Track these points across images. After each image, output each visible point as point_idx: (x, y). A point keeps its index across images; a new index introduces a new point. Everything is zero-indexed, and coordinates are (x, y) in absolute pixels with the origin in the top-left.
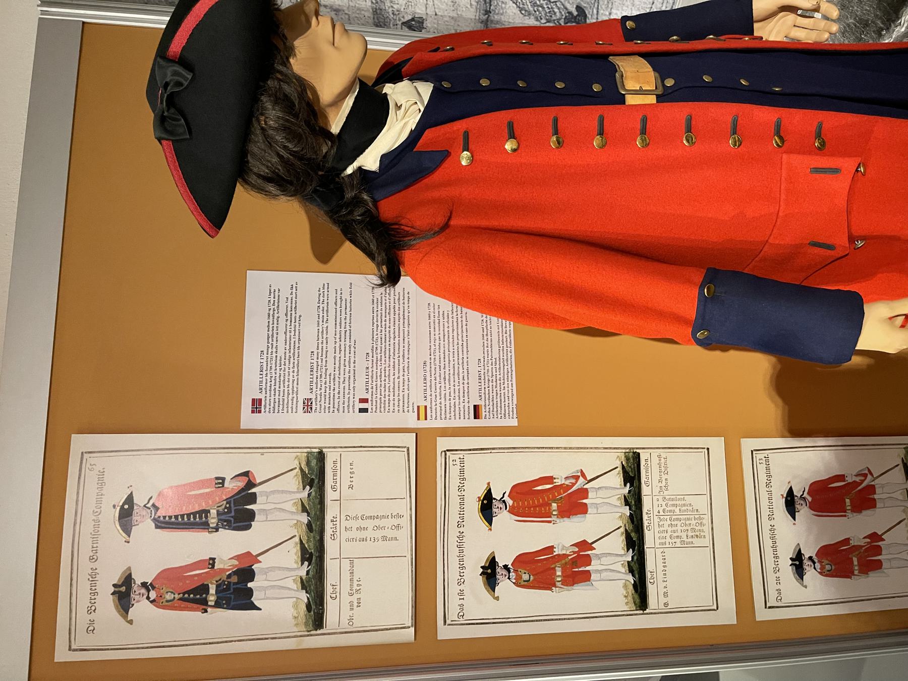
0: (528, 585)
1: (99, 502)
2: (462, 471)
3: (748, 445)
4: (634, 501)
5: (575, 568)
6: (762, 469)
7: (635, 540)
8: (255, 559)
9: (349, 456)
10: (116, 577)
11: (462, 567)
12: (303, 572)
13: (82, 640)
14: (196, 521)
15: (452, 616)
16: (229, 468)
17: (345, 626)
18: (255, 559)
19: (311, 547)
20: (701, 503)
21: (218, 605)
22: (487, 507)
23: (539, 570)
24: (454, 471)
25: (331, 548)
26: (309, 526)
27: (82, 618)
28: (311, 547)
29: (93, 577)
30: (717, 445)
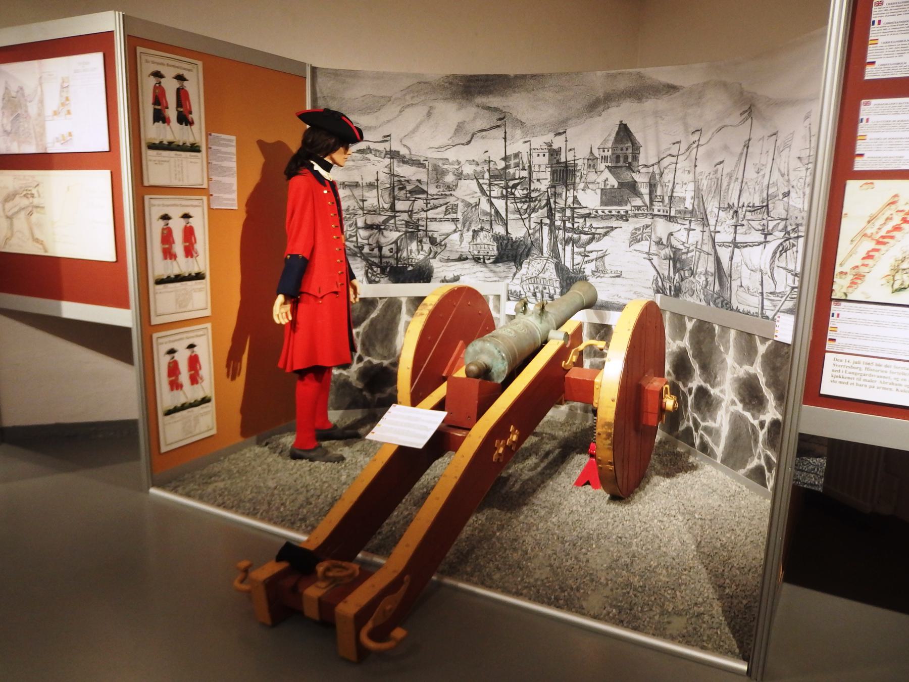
0: (163, 233)
1: (184, 69)
2: (196, 206)
3: (209, 326)
4: (190, 278)
5: (168, 254)
6: (201, 333)
7: (179, 278)
8: (169, 124)
9: (199, 161)
10: (163, 72)
11: (168, 206)
12: (165, 142)
13: (144, 57)
14: (179, 104)
15: (153, 202)
16: (194, 116)
17: (149, 158)
18: (169, 124)
19: (173, 146)
20: (189, 307)
21: (155, 109)
22: (186, 216)
23: (167, 238)
24: (196, 203)
25: (173, 153)
26: (179, 146)
27: (150, 59)
28: (173, 146)
29: (162, 64)
30: (208, 313)
